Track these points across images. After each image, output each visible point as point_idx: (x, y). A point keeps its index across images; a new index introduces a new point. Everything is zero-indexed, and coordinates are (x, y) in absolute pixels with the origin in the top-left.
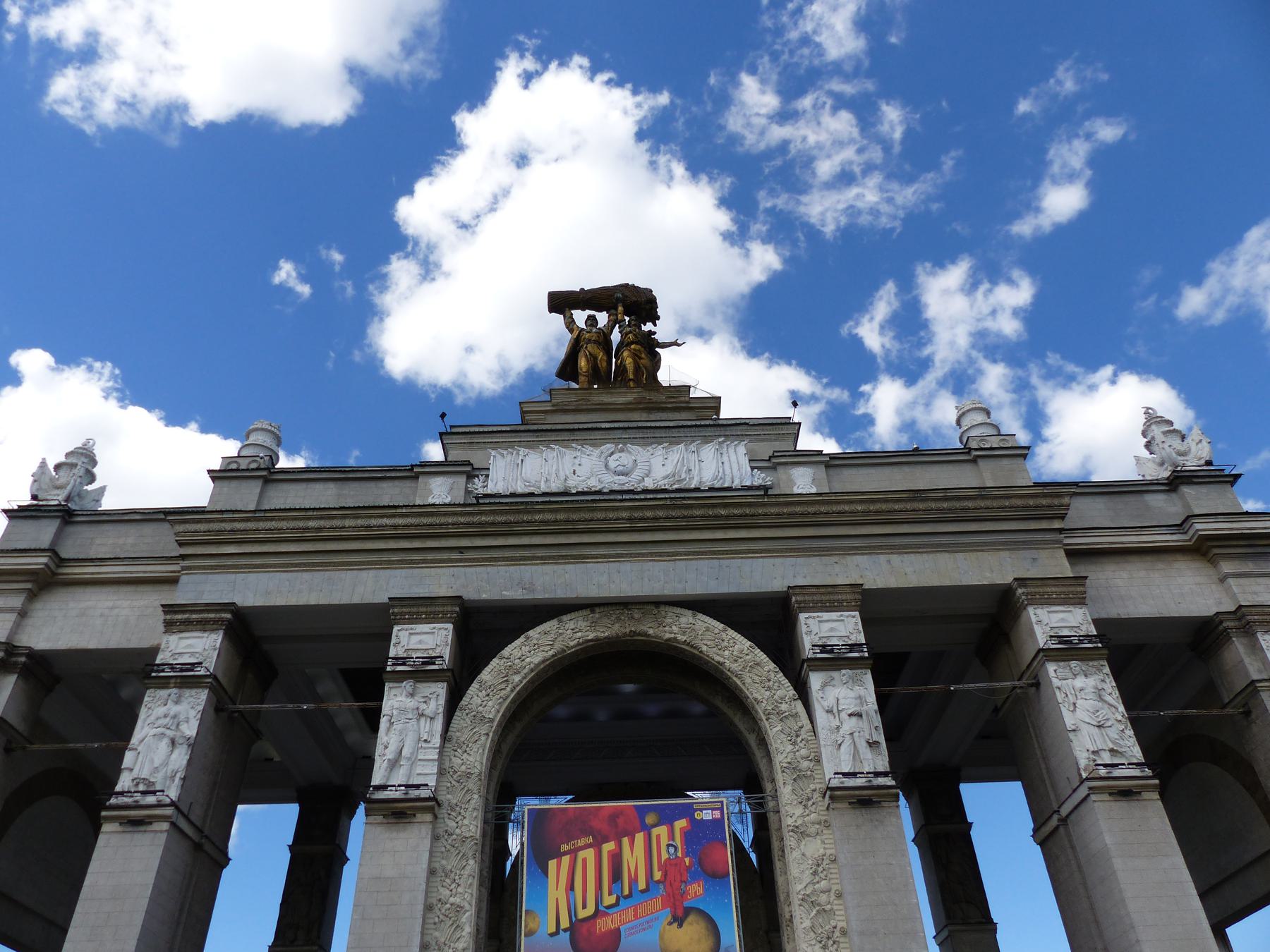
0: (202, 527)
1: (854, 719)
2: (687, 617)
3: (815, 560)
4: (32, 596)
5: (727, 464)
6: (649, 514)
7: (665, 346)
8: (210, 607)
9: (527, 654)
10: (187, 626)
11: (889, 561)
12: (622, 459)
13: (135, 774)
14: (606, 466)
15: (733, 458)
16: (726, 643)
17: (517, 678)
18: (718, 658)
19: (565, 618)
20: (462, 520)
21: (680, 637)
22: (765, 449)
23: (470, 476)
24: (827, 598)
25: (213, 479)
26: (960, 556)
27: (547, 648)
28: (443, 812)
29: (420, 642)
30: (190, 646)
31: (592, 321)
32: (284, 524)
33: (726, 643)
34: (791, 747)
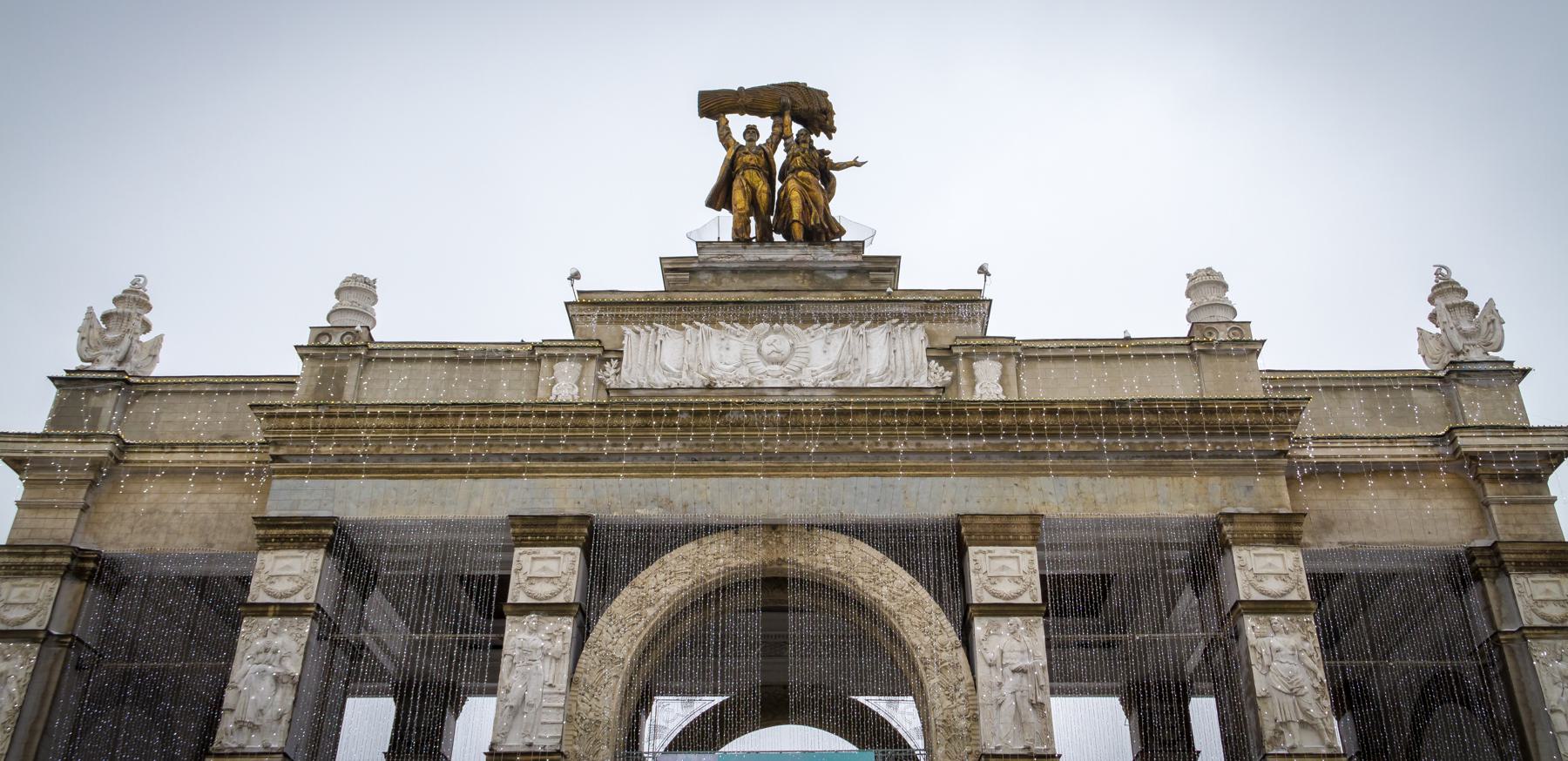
1: (1018, 676)
2: (842, 544)
5: (899, 354)
9: (666, 582)
10: (282, 542)
13: (238, 714)
14: (759, 351)
15: (907, 345)
16: (884, 578)
17: (650, 612)
18: (874, 595)
19: (705, 540)
21: (834, 568)
22: (948, 332)
23: (602, 361)
24: (1001, 531)
25: (302, 357)
27: (684, 577)
29: (544, 569)
30: (288, 567)
31: (751, 132)
33: (884, 578)
34: (948, 703)
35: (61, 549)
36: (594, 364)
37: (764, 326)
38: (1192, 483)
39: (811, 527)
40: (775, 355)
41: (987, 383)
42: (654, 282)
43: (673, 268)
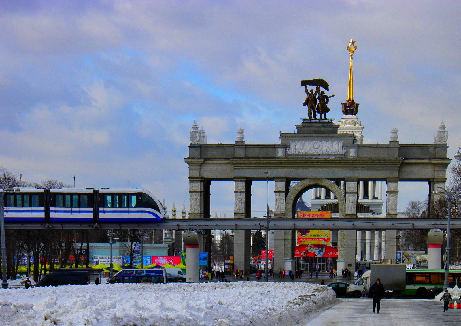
0: (237, 161)
2: (327, 181)
3: (352, 171)
4: (200, 166)
6: (321, 162)
7: (330, 97)
8: (242, 178)
11: (365, 172)
12: (316, 145)
17: (297, 192)
19: (305, 180)
20: (286, 161)
23: (286, 148)
26: (379, 171)
28: (286, 215)
31: (312, 91)
32: (252, 161)
35: (199, 178)
36: (284, 149)
37: (314, 142)
38: (384, 172)
39: (322, 178)
40: (316, 148)
41: (352, 153)
42: (294, 131)
43: (298, 126)
